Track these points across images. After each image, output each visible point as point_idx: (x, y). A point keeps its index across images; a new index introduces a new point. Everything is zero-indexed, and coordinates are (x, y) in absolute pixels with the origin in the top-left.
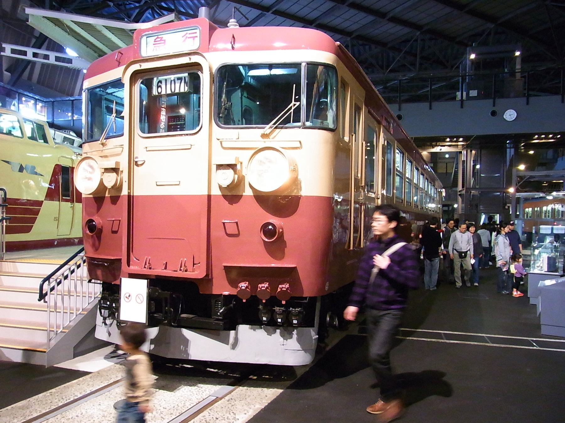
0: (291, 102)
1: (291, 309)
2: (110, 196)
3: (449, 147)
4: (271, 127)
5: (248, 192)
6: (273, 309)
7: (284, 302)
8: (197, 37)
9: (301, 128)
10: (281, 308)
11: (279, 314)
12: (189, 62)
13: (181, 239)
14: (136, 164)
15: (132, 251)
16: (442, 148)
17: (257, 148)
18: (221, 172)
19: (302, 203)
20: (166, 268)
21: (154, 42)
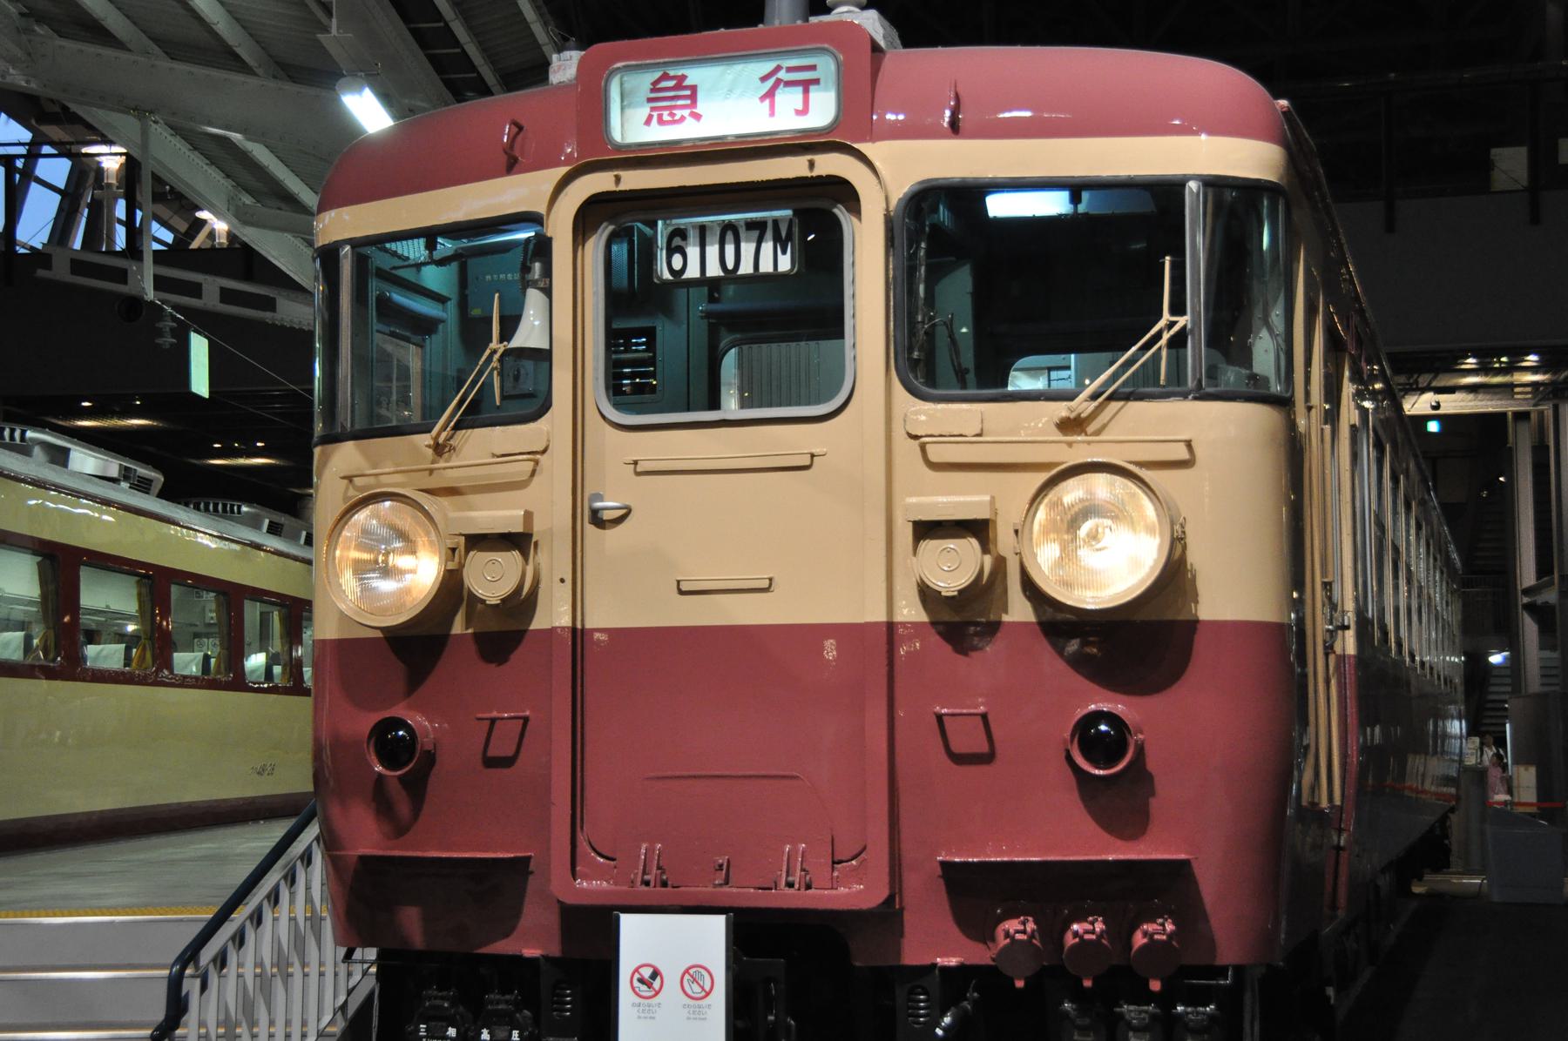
0: (1160, 316)
1: (1180, 1009)
2: (475, 634)
3: (1471, 396)
4: (1094, 397)
5: (1019, 610)
6: (1118, 1010)
7: (1155, 985)
8: (816, 82)
9: (1190, 397)
10: (1146, 1008)
11: (1136, 1030)
12: (809, 174)
13: (784, 777)
14: (597, 520)
15: (582, 828)
16: (1442, 398)
17: (1063, 463)
18: (929, 546)
19: (1202, 647)
20: (727, 882)
21: (652, 91)
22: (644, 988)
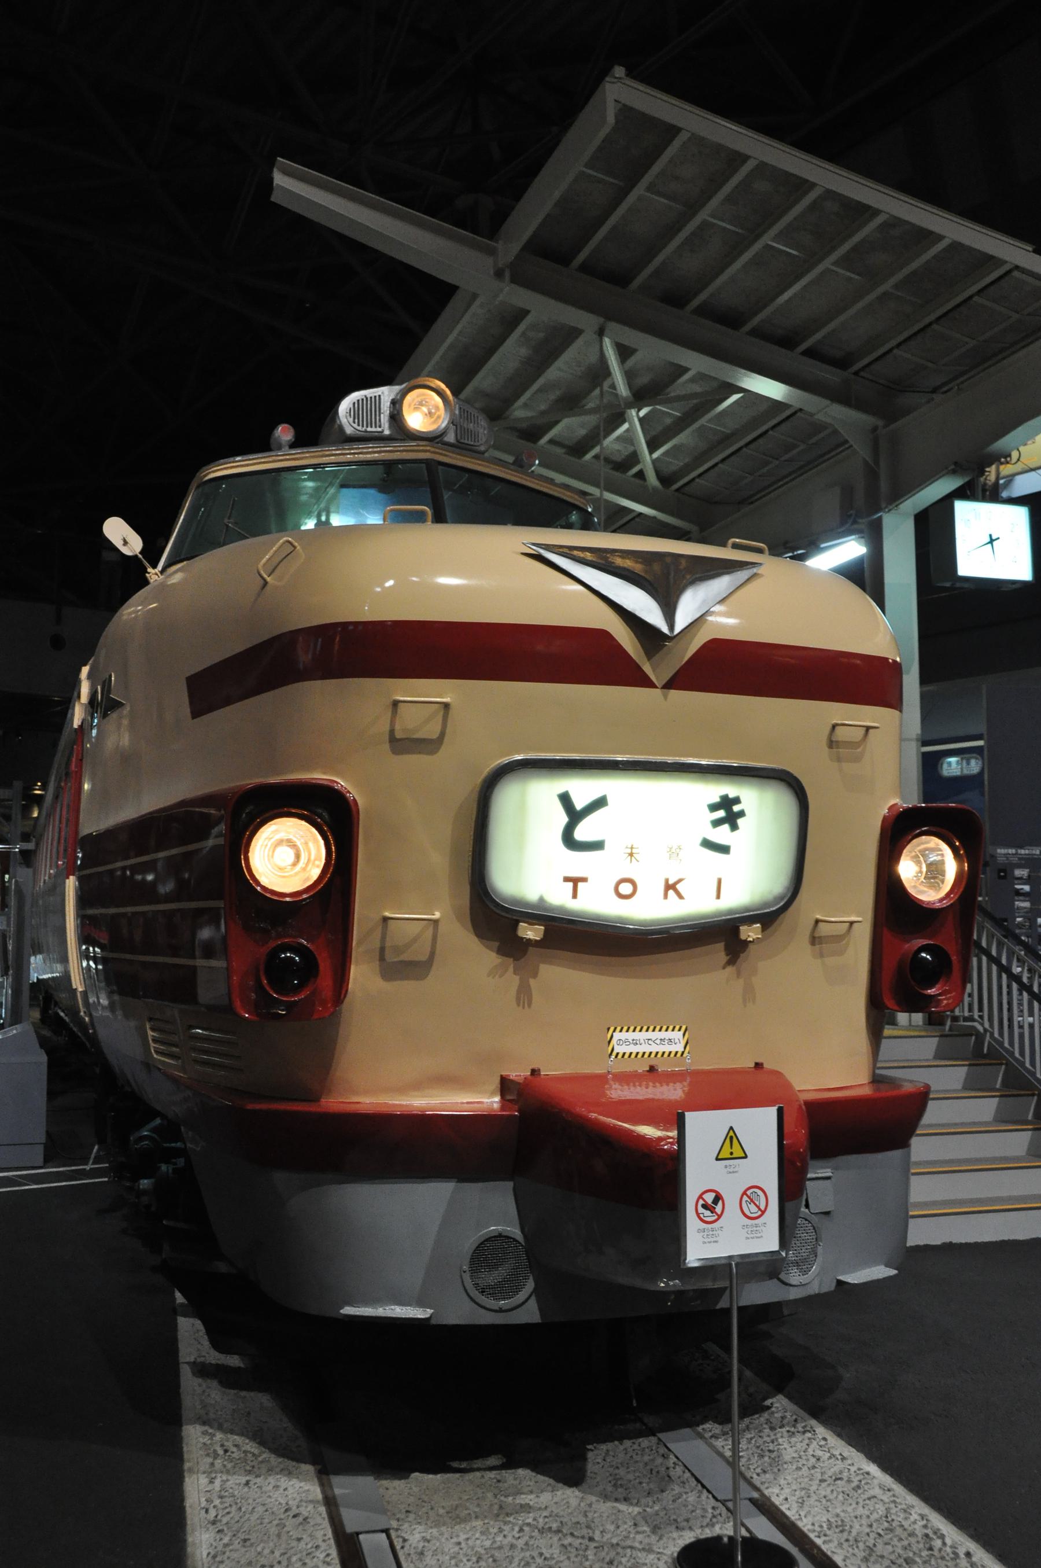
22: (708, 1213)
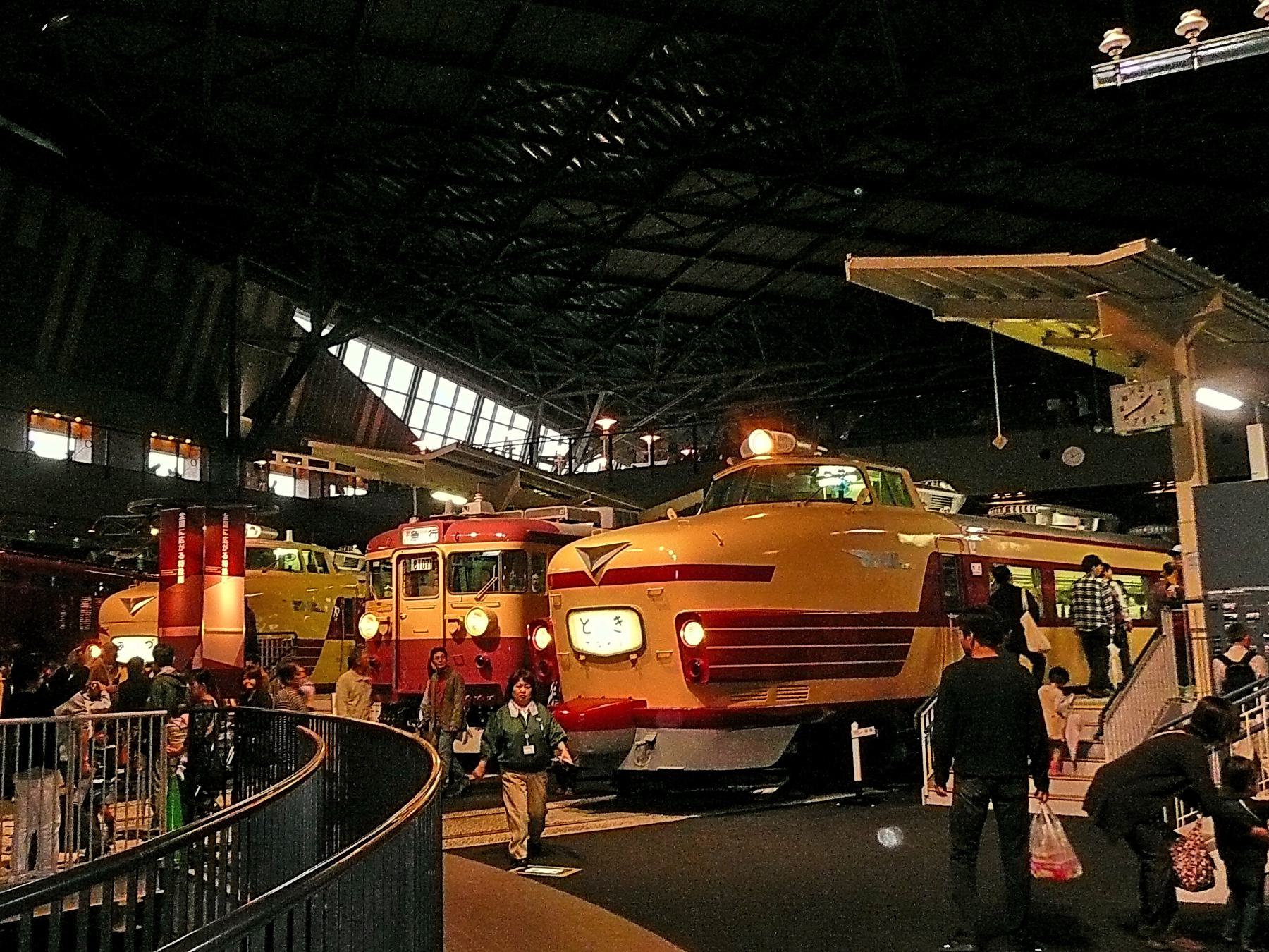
14: (401, 618)
